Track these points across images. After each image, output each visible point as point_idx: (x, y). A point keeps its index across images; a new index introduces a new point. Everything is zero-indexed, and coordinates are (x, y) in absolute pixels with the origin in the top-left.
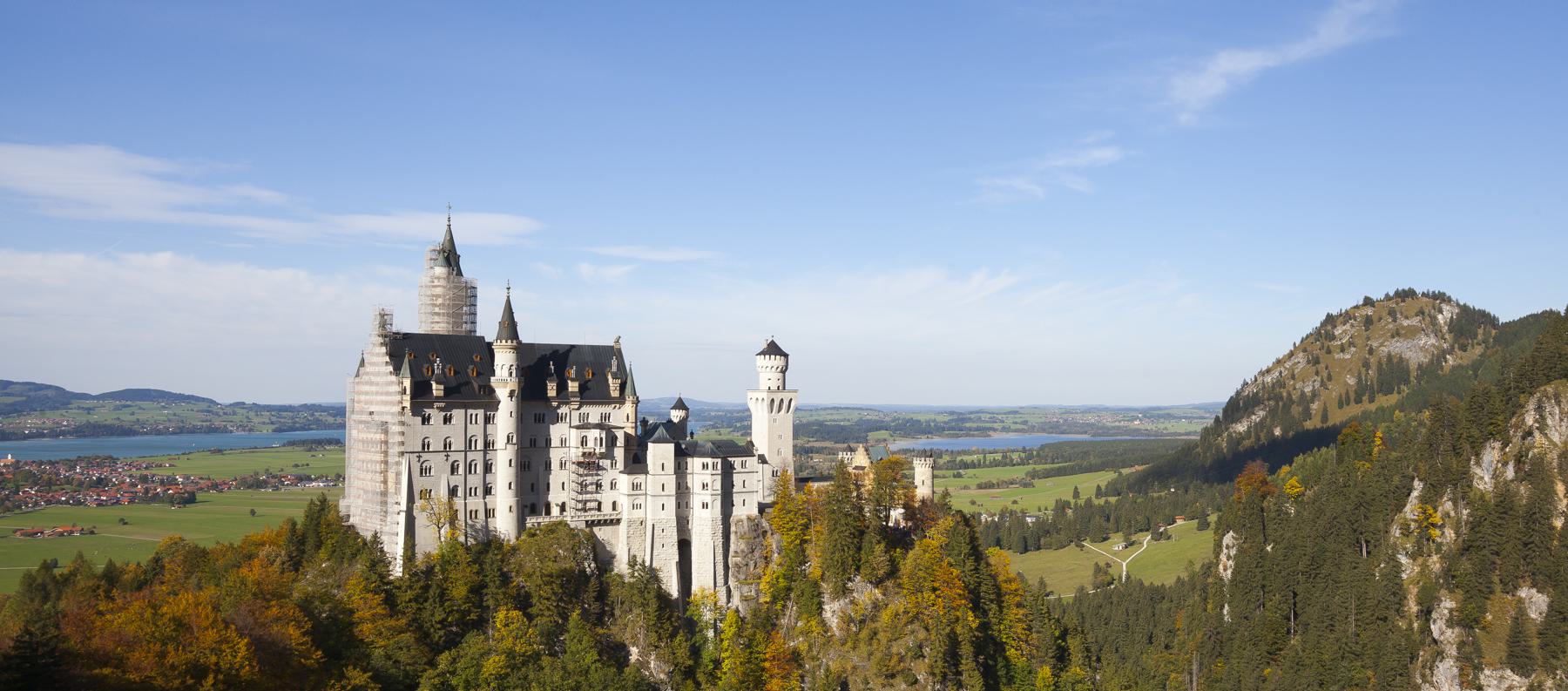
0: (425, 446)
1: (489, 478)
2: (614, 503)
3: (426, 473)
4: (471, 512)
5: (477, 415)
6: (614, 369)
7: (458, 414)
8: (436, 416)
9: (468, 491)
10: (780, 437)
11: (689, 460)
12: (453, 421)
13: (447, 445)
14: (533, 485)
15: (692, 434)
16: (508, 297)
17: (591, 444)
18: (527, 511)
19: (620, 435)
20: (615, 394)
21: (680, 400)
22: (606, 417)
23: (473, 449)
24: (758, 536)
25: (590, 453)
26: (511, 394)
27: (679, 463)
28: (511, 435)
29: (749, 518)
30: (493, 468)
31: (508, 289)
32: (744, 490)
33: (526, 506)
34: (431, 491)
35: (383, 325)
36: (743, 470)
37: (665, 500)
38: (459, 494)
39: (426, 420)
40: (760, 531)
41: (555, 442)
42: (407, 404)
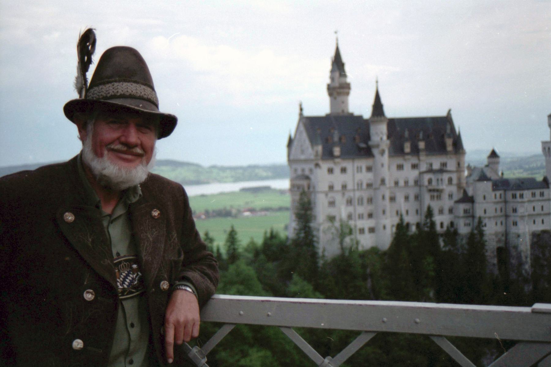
0: (331, 188)
6: (448, 131)
8: (337, 170)
9: (357, 216)
11: (502, 192)
13: (344, 187)
15: (502, 174)
17: (434, 183)
19: (454, 176)
20: (450, 148)
22: (444, 165)
27: (495, 195)
31: (377, 82)
32: (542, 212)
35: (301, 109)
36: (541, 198)
38: (353, 217)
39: (331, 171)
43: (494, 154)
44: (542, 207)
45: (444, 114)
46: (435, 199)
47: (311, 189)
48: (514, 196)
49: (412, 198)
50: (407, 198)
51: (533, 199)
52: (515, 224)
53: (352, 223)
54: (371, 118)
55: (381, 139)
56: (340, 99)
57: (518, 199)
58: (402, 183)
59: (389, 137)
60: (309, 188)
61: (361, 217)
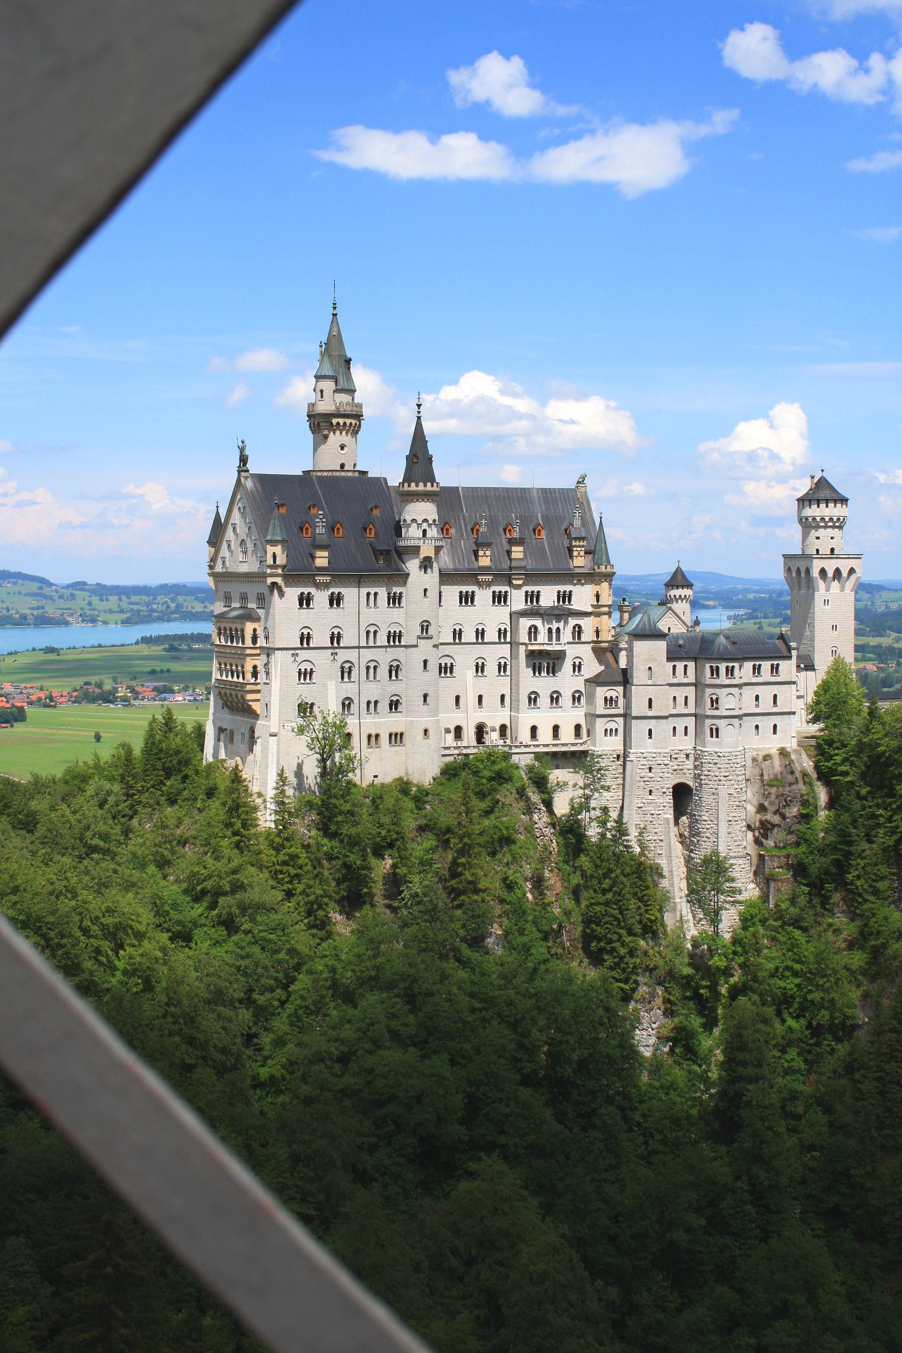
0: (305, 639)
1: (394, 688)
2: (578, 728)
3: (305, 679)
4: (369, 736)
5: (376, 594)
6: (577, 523)
7: (350, 594)
8: (321, 597)
9: (364, 706)
10: (835, 628)
12: (345, 603)
13: (336, 638)
14: (457, 698)
16: (419, 418)
17: (542, 637)
18: (450, 739)
21: (678, 571)
22: (565, 597)
23: (371, 644)
24: (797, 782)
25: (540, 652)
26: (426, 564)
27: (674, 667)
28: (425, 624)
29: (783, 753)
30: (400, 673)
31: (419, 406)
32: (775, 710)
33: (448, 731)
34: (312, 705)
35: (244, 460)
37: (652, 724)
38: (354, 708)
39: (305, 601)
40: (798, 774)
41: (491, 635)
42: (279, 580)
43: (678, 580)
44: (775, 696)
45: (569, 483)
46: (544, 674)
47: (261, 642)
48: (715, 672)
49: (491, 668)
50: (480, 668)
51: (755, 680)
52: (715, 732)
53: (352, 725)
54: (403, 483)
55: (425, 532)
56: (335, 439)
57: (723, 679)
58: (469, 636)
59: (444, 528)
60: (255, 639)
61: (372, 705)
